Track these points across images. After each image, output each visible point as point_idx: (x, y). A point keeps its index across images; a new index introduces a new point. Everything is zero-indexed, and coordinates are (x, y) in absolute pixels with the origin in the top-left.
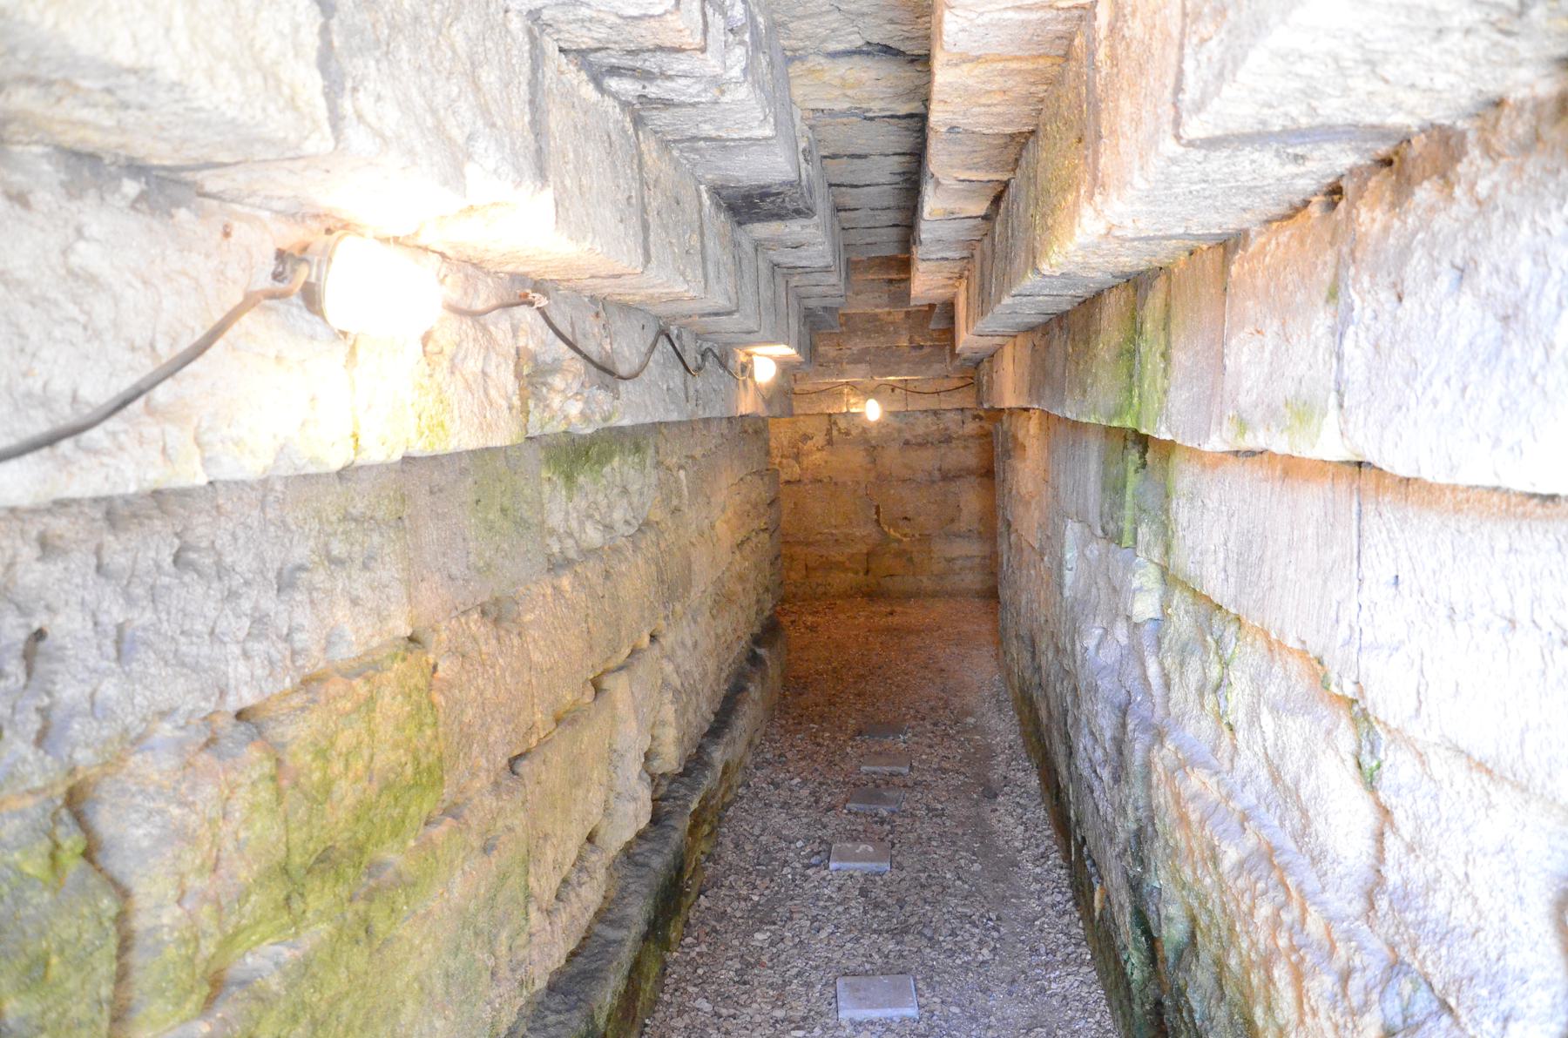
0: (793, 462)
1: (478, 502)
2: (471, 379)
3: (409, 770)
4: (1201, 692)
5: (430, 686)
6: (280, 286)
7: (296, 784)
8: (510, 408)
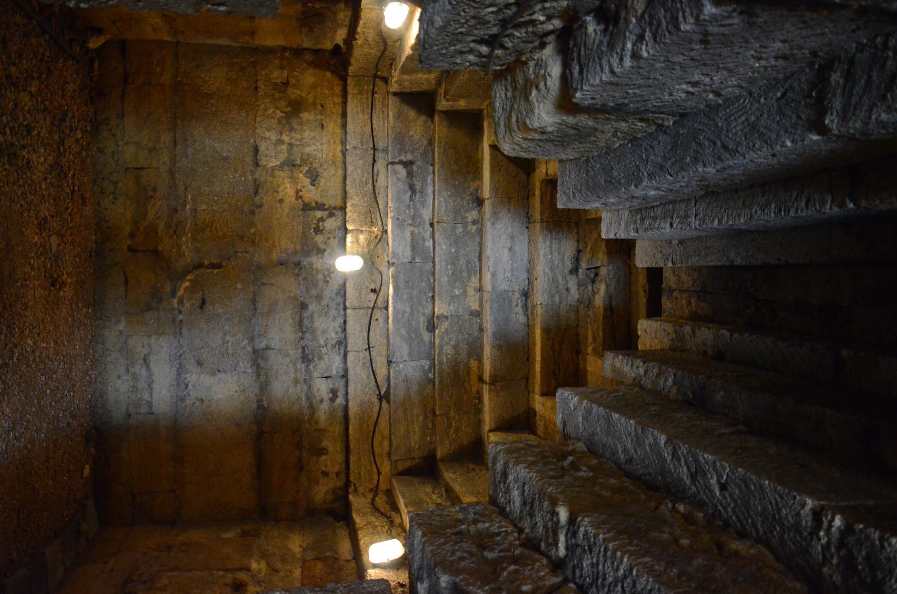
0: (283, 157)
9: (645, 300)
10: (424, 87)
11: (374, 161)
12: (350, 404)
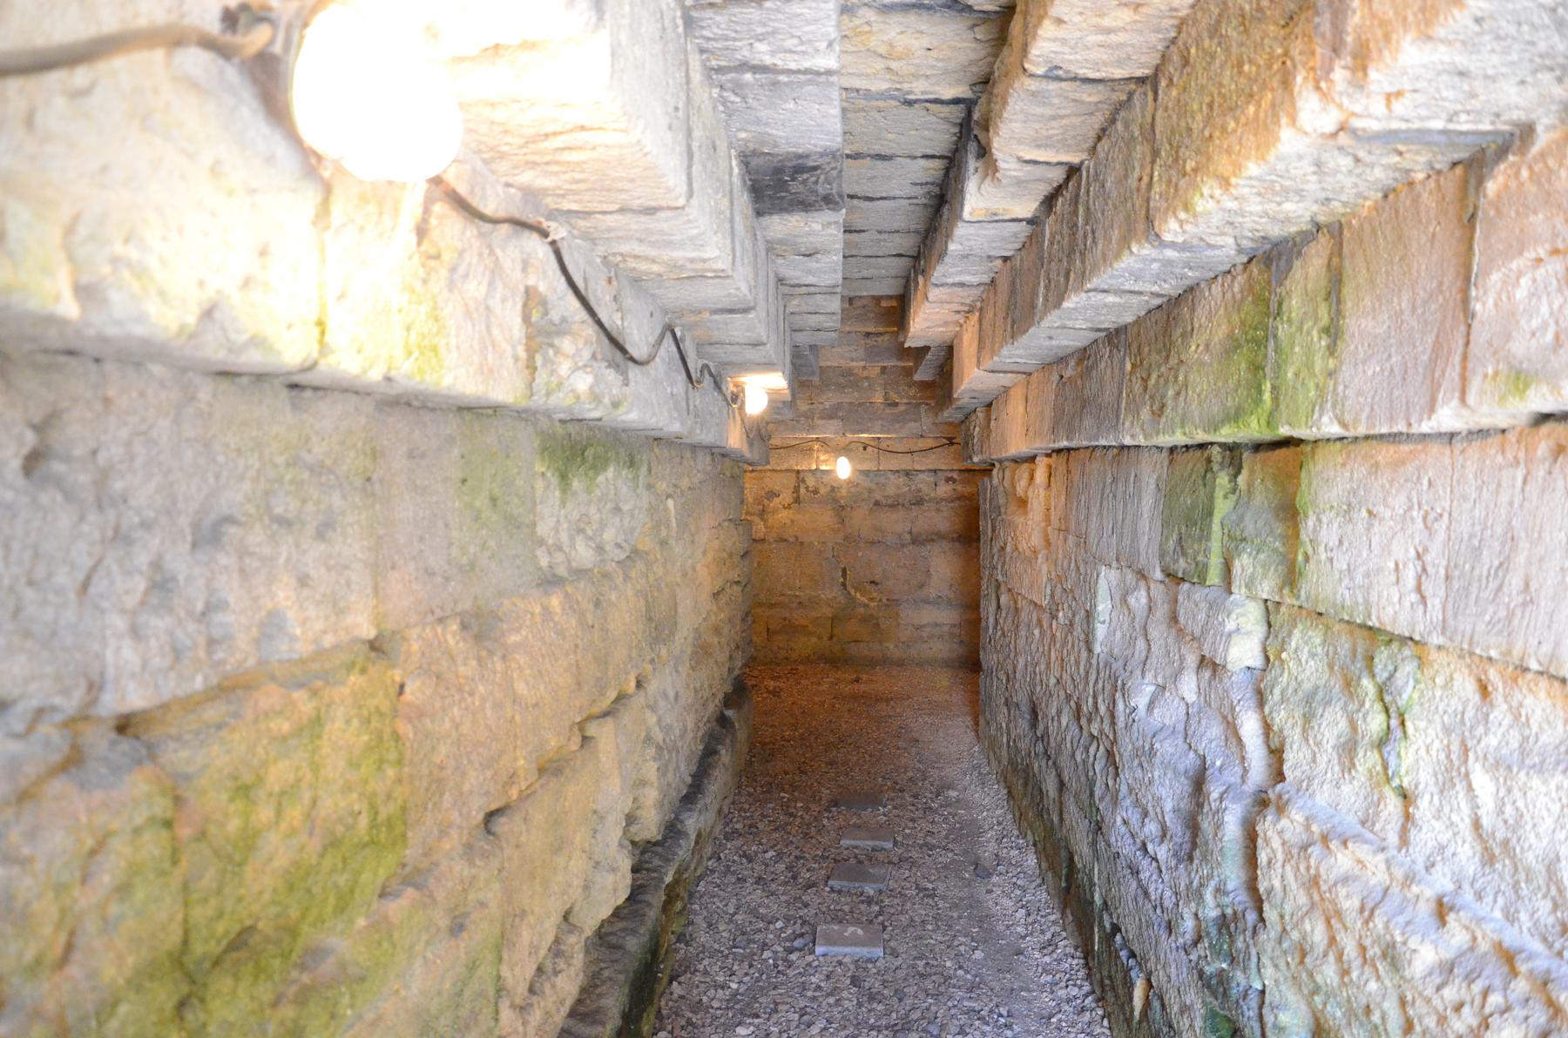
0: (756, 519)
1: (464, 481)
2: (471, 303)
3: (364, 821)
4: (1348, 749)
5: (395, 713)
6: (228, 38)
7: (202, 835)
8: (516, 359)
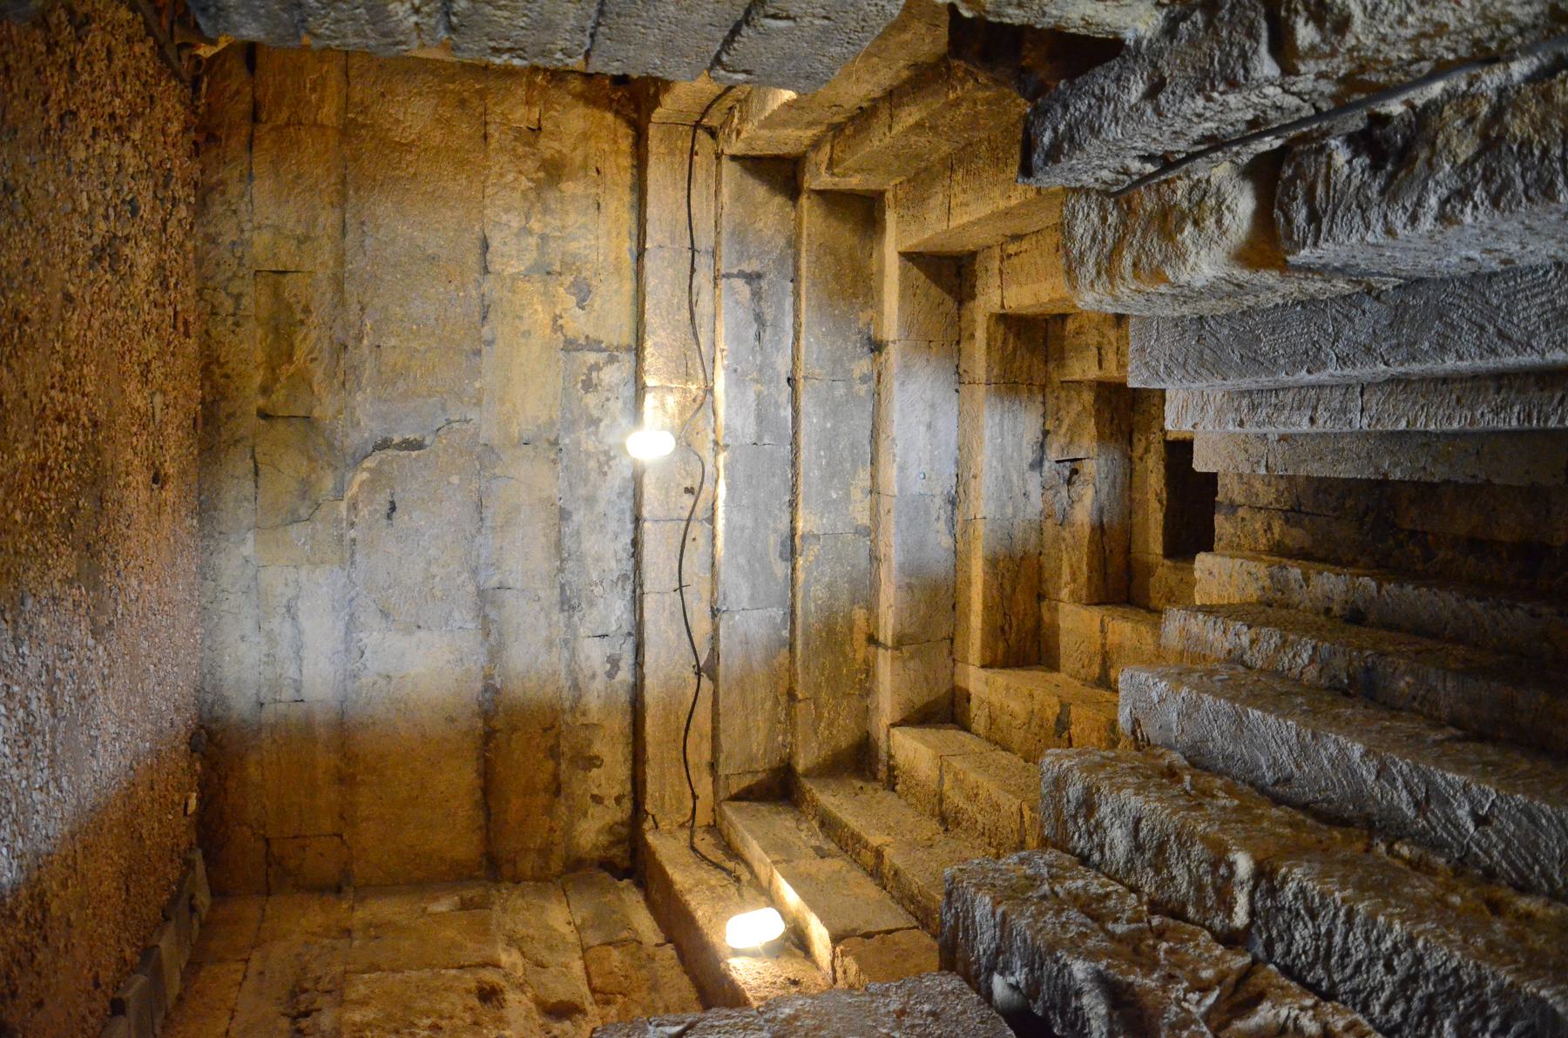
0: (530, 257)
9: (1160, 516)
10: (785, 150)
11: (693, 270)
12: (648, 682)
